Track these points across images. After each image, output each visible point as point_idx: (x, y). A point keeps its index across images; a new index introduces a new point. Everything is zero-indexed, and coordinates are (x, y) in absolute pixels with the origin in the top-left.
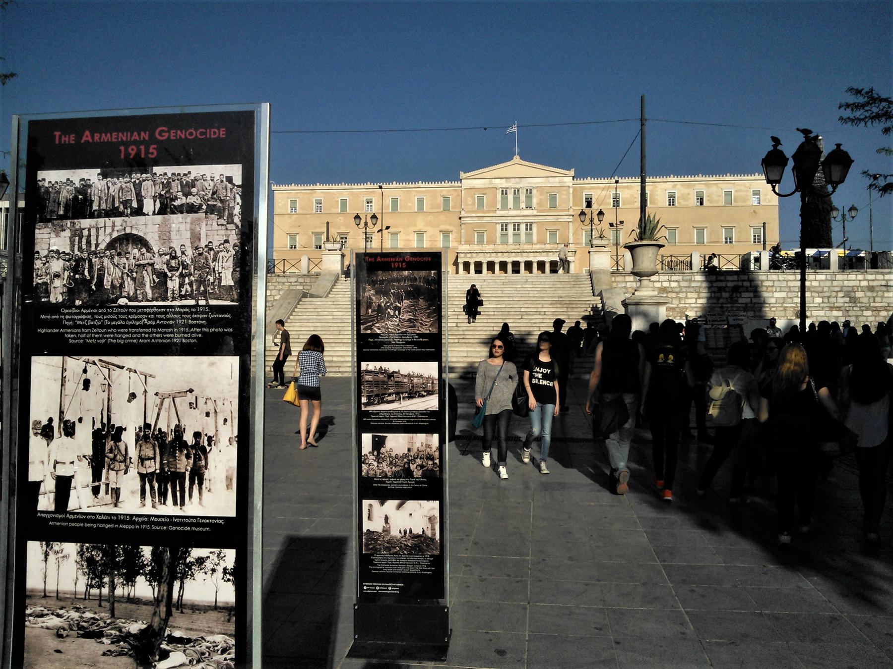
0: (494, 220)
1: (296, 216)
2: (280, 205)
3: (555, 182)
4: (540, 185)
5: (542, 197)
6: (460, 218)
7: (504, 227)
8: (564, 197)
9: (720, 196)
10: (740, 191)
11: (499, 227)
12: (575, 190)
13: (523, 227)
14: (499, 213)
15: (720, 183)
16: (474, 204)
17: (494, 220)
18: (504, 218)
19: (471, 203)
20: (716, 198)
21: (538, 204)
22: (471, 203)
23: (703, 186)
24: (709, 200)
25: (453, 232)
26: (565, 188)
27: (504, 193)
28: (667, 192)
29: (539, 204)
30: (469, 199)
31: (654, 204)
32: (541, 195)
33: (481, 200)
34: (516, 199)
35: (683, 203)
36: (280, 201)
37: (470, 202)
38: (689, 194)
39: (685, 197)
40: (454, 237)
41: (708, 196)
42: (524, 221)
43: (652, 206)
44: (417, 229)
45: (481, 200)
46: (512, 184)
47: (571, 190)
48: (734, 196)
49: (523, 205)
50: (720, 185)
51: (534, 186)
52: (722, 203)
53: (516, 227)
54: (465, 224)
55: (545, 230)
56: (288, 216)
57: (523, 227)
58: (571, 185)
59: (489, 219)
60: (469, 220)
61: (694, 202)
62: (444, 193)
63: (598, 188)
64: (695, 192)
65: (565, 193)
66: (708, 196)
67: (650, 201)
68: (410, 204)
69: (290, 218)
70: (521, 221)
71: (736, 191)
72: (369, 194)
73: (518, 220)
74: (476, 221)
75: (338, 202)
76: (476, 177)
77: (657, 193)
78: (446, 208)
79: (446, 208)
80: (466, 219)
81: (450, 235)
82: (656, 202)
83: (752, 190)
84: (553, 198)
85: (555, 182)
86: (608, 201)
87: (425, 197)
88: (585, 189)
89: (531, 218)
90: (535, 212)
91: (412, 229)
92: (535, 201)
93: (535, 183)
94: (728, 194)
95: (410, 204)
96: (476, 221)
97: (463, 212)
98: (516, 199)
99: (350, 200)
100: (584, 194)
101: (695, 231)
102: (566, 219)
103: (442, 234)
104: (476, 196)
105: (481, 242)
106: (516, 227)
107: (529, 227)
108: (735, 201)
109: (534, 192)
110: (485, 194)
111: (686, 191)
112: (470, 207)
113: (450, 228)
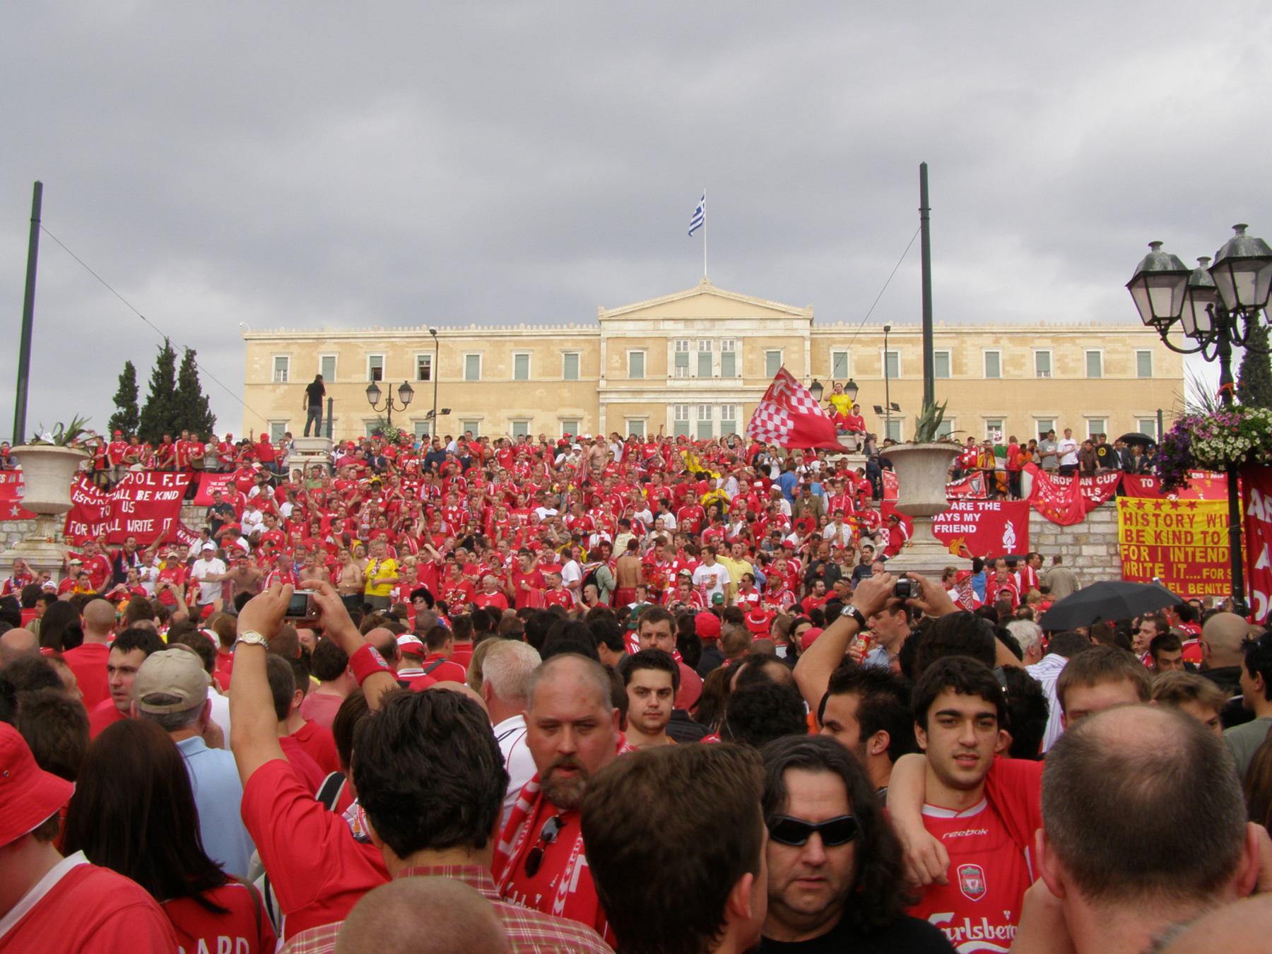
0: (663, 399)
1: (286, 387)
2: (257, 366)
3: (777, 328)
4: (749, 334)
5: (750, 356)
6: (599, 392)
8: (794, 356)
9: (1079, 360)
10: (1115, 351)
12: (813, 342)
15: (1079, 338)
16: (623, 367)
17: (663, 399)
18: (681, 395)
19: (618, 365)
20: (1071, 365)
22: (618, 365)
23: (1049, 340)
24: (1059, 368)
25: (585, 421)
28: (984, 351)
29: (750, 370)
30: (616, 358)
31: (961, 372)
33: (637, 357)
35: (1014, 373)
36: (256, 359)
37: (614, 363)
38: (1023, 356)
39: (1017, 362)
41: (1059, 360)
42: (720, 401)
43: (958, 377)
45: (637, 357)
46: (696, 330)
47: (808, 344)
48: (1105, 361)
49: (716, 371)
50: (1078, 341)
52: (1082, 373)
54: (603, 404)
56: (271, 387)
59: (652, 395)
60: (613, 398)
61: (1030, 369)
62: (568, 346)
63: (860, 342)
64: (1034, 351)
65: (795, 349)
66: (1059, 360)
67: (954, 367)
68: (501, 366)
69: (274, 391)
70: (713, 401)
71: (1108, 352)
72: (425, 346)
73: (708, 398)
74: (629, 399)
75: (365, 361)
76: (629, 317)
77: (965, 353)
78: (571, 373)
79: (571, 373)
80: (608, 396)
81: (579, 425)
82: (965, 369)
83: (1136, 351)
85: (777, 328)
86: (876, 365)
87: (530, 354)
88: (833, 342)
89: (732, 395)
90: (739, 384)
91: (505, 413)
92: (739, 362)
94: (1093, 357)
95: (501, 366)
96: (629, 399)
97: (603, 384)
98: (705, 359)
99: (386, 358)
100: (832, 352)
101: (1037, 423)
103: (562, 424)
104: (628, 353)
108: (1107, 371)
110: (646, 349)
111: (1018, 350)
112: (617, 372)
113: (578, 412)
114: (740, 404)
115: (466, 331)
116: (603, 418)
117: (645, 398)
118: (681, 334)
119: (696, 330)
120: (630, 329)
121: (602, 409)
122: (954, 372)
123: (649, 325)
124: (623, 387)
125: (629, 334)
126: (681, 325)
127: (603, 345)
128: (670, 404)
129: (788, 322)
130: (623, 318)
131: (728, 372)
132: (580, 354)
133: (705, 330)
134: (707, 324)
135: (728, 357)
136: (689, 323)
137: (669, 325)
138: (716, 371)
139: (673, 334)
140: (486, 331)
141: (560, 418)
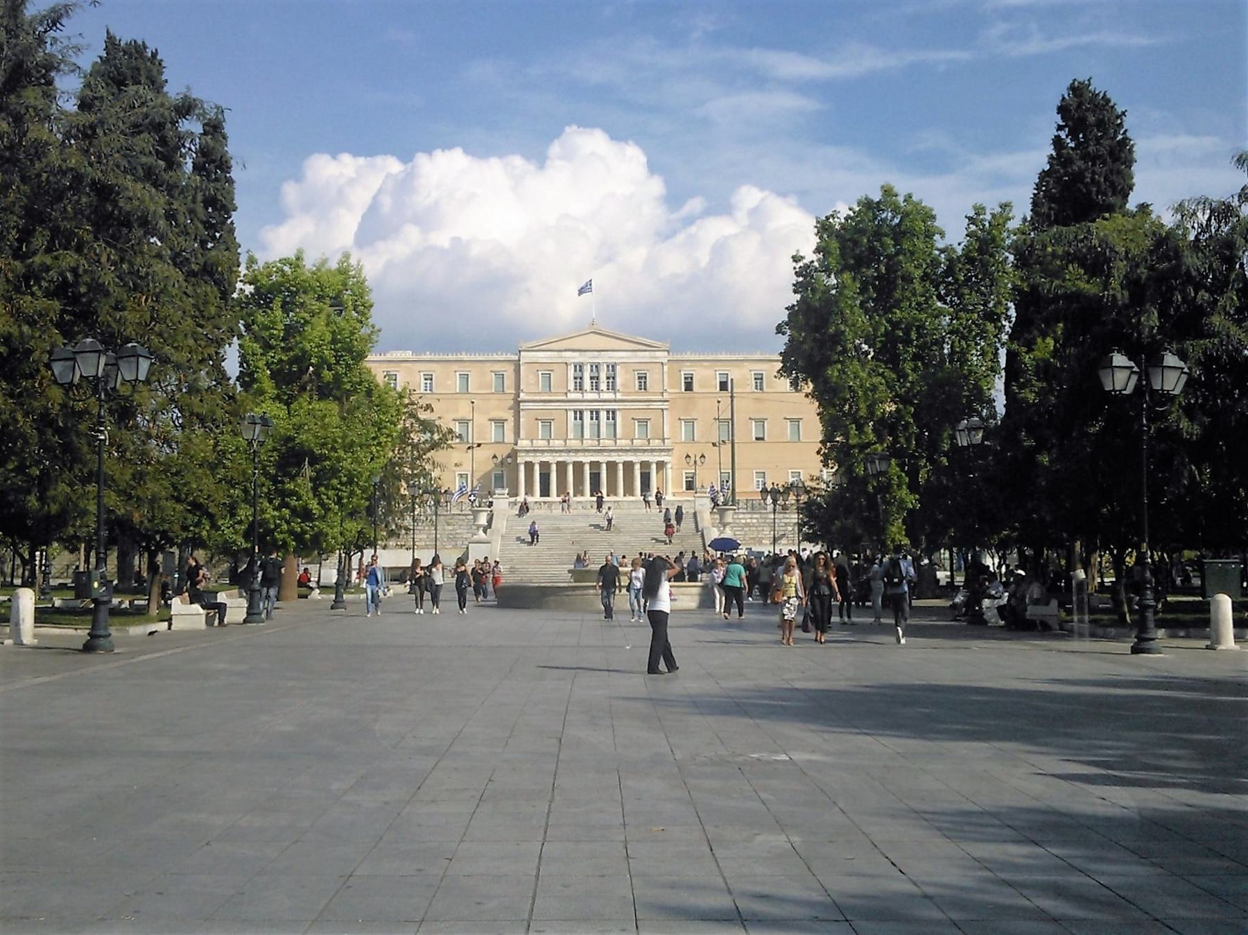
3: (645, 356)
6: (520, 402)
7: (579, 414)
11: (571, 414)
14: (571, 396)
19: (532, 382)
21: (623, 385)
22: (532, 382)
27: (579, 367)
30: (531, 377)
34: (595, 379)
44: (459, 416)
49: (603, 386)
51: (617, 361)
53: (596, 414)
58: (665, 361)
68: (449, 382)
84: (642, 378)
90: (619, 396)
92: (619, 381)
95: (449, 382)
97: (522, 395)
100: (682, 373)
106: (596, 414)
107: (612, 414)
114: (619, 409)
115: (423, 357)
120: (541, 356)
122: (767, 387)
124: (537, 398)
128: (570, 410)
130: (536, 348)
131: (612, 387)
135: (612, 378)
138: (603, 386)
140: (437, 357)
141: (490, 420)
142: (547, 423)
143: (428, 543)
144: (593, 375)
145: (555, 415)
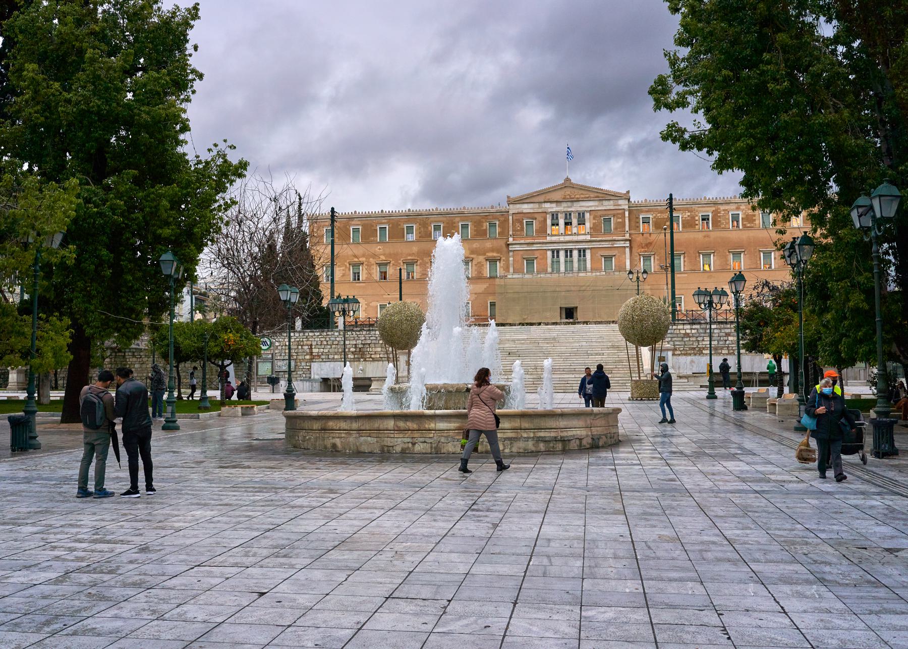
6: (509, 245)
11: (549, 254)
13: (575, 253)
18: (555, 245)
26: (620, 212)
27: (555, 216)
32: (594, 219)
40: (502, 265)
46: (563, 207)
47: (627, 214)
55: (600, 257)
57: (575, 253)
60: (517, 248)
73: (570, 246)
93: (588, 207)
97: (511, 239)
100: (641, 217)
102: (621, 244)
105: (530, 271)
107: (583, 252)
109: (587, 215)
114: (589, 248)
116: (511, 259)
117: (534, 247)
118: (554, 210)
119: (563, 207)
120: (526, 208)
121: (511, 254)
123: (537, 205)
125: (525, 211)
126: (554, 205)
127: (511, 217)
129: (616, 201)
132: (497, 223)
133: (569, 207)
134: (569, 204)
136: (559, 204)
137: (547, 205)
139: (550, 210)
142: (530, 261)
143: (381, 356)
144: (567, 221)
145: (537, 254)
